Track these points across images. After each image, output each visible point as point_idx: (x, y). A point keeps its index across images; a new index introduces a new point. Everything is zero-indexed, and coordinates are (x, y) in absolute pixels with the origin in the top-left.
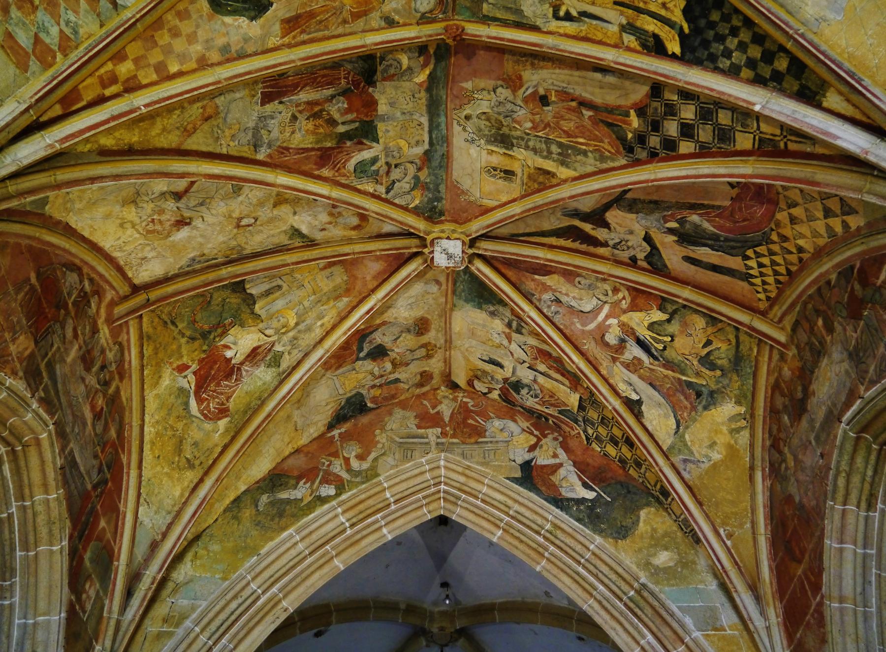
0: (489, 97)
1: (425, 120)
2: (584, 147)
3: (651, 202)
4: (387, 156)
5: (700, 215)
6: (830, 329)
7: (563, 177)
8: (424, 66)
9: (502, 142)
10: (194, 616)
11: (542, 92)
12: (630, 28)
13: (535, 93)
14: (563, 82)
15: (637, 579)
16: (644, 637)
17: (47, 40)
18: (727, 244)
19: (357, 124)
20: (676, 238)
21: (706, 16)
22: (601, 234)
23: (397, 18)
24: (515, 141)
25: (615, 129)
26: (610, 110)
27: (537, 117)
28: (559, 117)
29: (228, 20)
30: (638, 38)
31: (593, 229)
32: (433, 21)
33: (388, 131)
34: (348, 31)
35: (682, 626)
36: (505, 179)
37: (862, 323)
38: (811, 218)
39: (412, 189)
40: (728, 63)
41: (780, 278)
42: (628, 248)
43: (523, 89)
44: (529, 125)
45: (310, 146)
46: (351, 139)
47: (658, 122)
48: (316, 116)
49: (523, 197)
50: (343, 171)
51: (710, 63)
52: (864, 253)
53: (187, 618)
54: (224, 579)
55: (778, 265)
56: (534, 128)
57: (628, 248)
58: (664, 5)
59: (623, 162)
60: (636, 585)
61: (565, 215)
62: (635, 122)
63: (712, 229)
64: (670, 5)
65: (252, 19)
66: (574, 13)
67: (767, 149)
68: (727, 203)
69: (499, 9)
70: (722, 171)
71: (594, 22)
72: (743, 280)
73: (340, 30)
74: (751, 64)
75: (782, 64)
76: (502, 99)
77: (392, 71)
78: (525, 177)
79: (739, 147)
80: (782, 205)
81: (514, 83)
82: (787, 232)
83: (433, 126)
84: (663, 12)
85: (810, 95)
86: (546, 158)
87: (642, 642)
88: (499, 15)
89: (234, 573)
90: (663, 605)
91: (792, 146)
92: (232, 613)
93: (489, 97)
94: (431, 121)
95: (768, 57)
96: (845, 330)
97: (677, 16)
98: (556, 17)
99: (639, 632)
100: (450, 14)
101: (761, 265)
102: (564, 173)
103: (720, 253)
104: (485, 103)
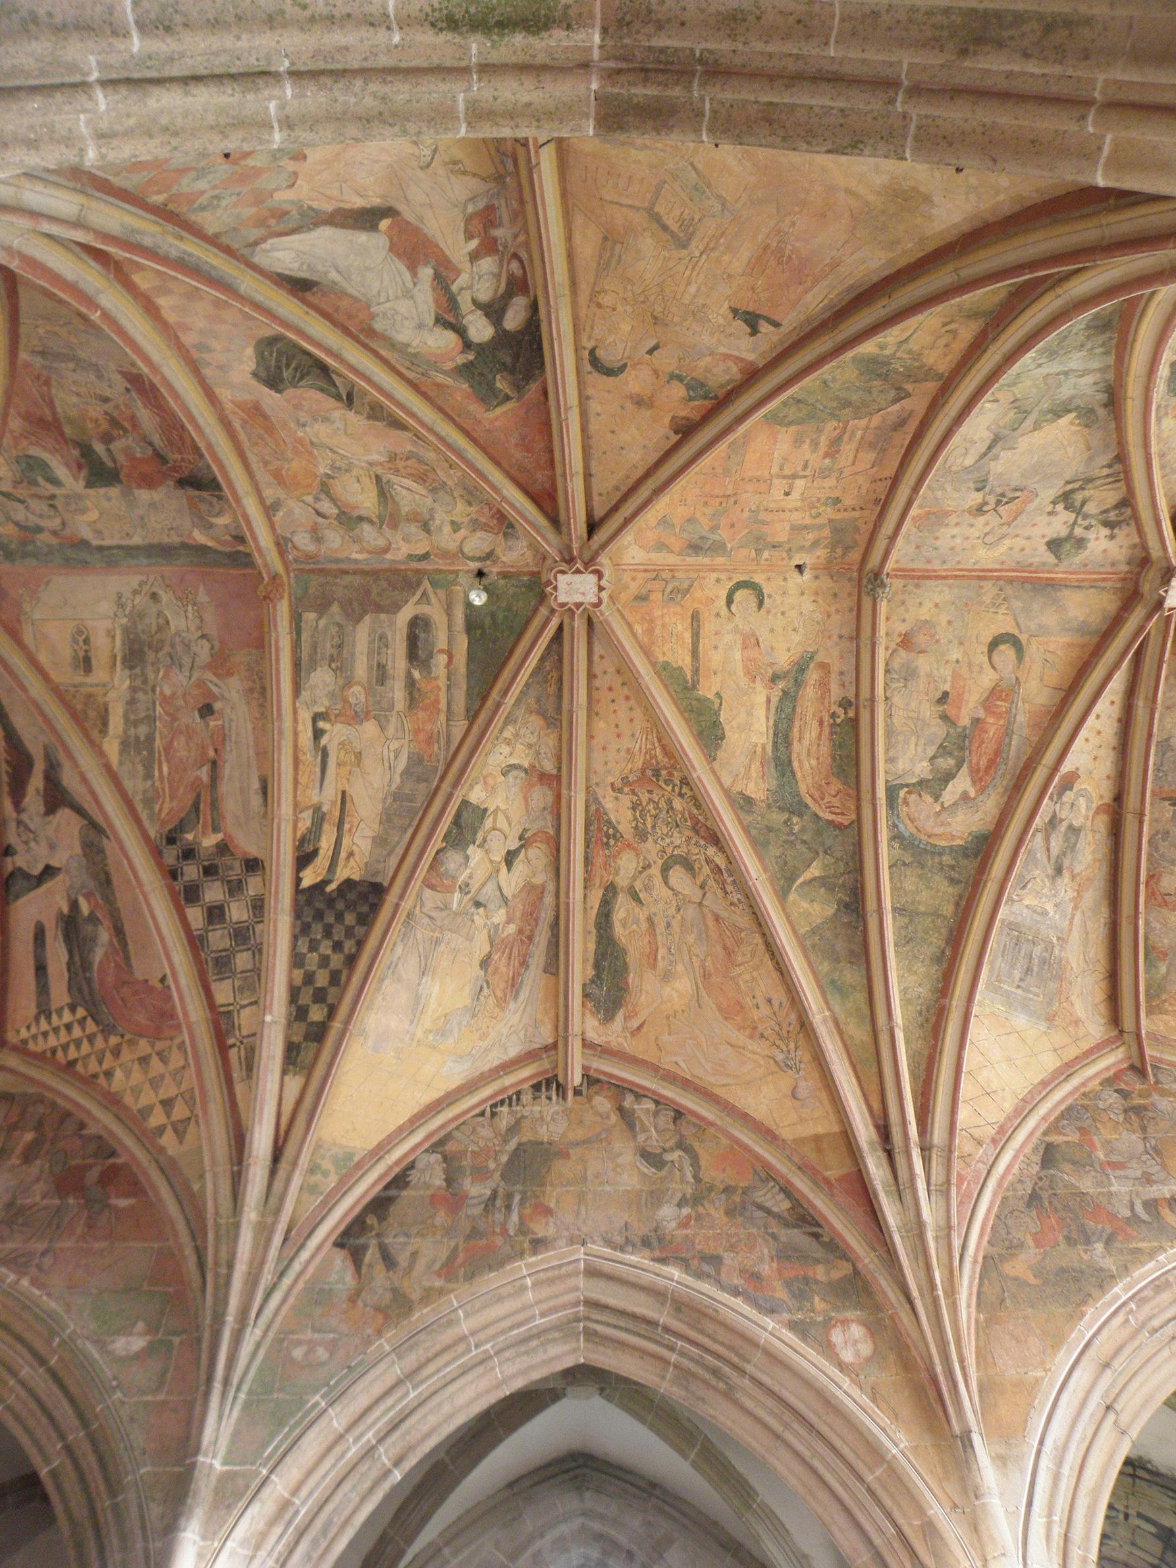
0: (192, 629)
1: (137, 540)
2: (156, 773)
3: (107, 874)
4: (66, 496)
5: (111, 943)
6: (29, 1156)
7: (106, 747)
8: (218, 541)
9: (132, 652)
11: (217, 706)
12: (319, 818)
13: (215, 698)
14: (237, 734)
17: (185, 181)
18: (84, 983)
19: (110, 464)
20: (66, 910)
21: (348, 907)
22: (33, 800)
23: (281, 514)
24: (138, 671)
25: (193, 816)
26: (215, 805)
27: (181, 702)
28: (189, 734)
29: (250, 351)
30: (309, 831)
31: (37, 791)
32: (282, 553)
33: (109, 499)
34: (255, 466)
36: (75, 658)
37: (57, 1201)
38: (155, 1083)
39: (17, 524)
40: (304, 950)
41: (60, 1054)
42: (26, 843)
43: (215, 679)
44: (168, 691)
45: (59, 410)
46: (83, 455)
47: (217, 873)
48: (114, 422)
49: (56, 691)
50: (25, 443)
51: (302, 929)
52: (138, 1164)
55: (78, 1047)
56: (165, 700)
57: (26, 843)
58: (351, 854)
59: (152, 833)
61: (45, 748)
62: (209, 841)
63: (97, 960)
64: (352, 862)
65: (255, 374)
66: (323, 741)
67: (222, 1025)
68: (139, 975)
69: (312, 636)
70: (183, 981)
71: (318, 770)
72: (39, 1006)
73: (252, 459)
74: (309, 979)
75: (317, 1014)
76: (194, 648)
77: (203, 507)
78: (90, 690)
79: (215, 987)
80: (160, 1045)
81: (220, 664)
82: (127, 1055)
83: (131, 551)
84: (343, 855)
85: (292, 1053)
86: (126, 717)
88: (304, 636)
91: (233, 1054)
93: (192, 629)
94: (137, 548)
95: (320, 996)
96: (38, 1179)
97: (342, 874)
98: (316, 718)
100: (295, 566)
101: (68, 1027)
102: (112, 748)
103: (66, 975)
104: (182, 624)
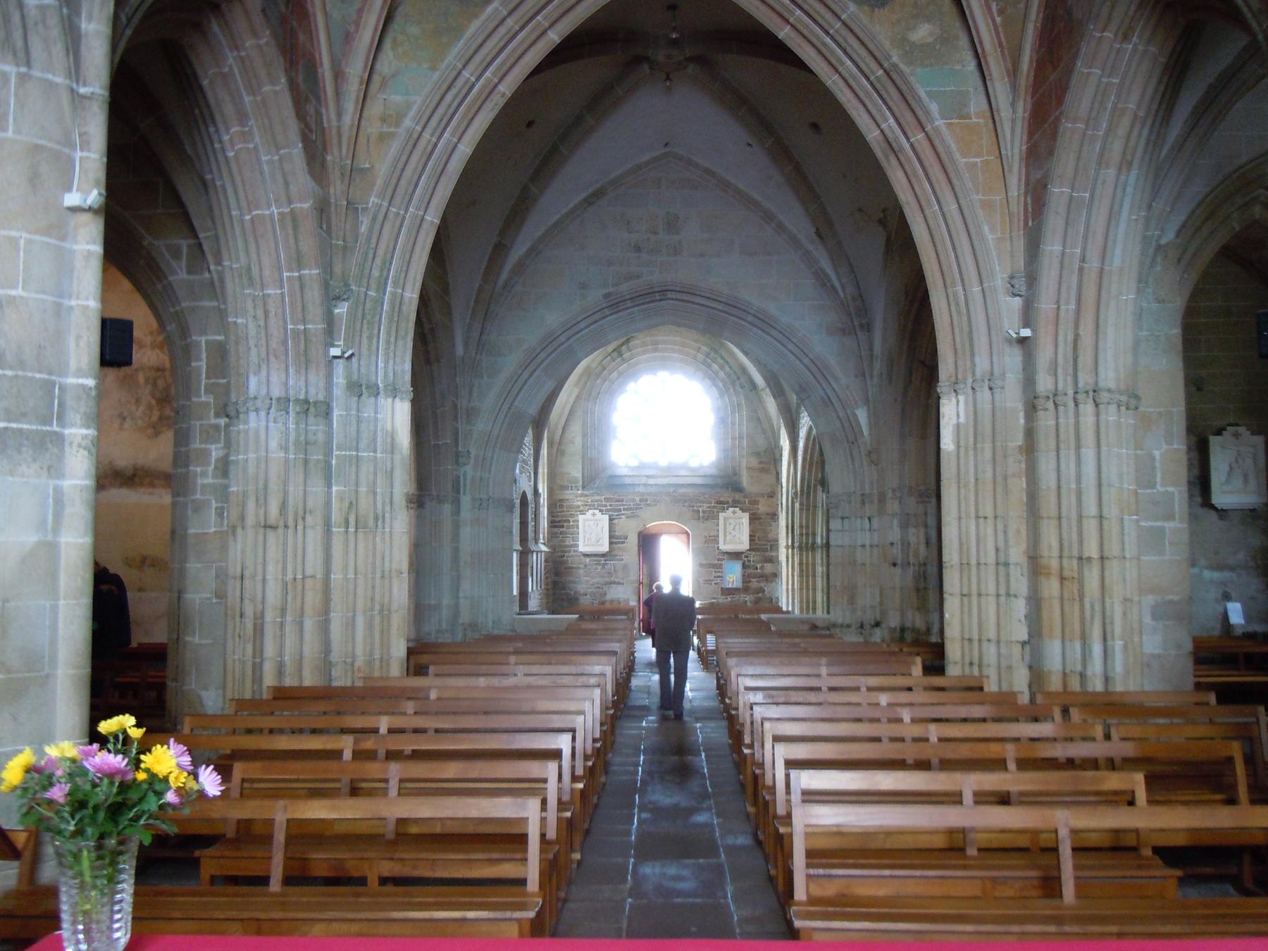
10: (412, 114)
15: (888, 57)
16: (886, 120)
35: (927, 113)
53: (405, 116)
54: (433, 69)
60: (886, 65)
87: (883, 126)
89: (443, 61)
90: (911, 89)
92: (450, 106)
99: (883, 115)
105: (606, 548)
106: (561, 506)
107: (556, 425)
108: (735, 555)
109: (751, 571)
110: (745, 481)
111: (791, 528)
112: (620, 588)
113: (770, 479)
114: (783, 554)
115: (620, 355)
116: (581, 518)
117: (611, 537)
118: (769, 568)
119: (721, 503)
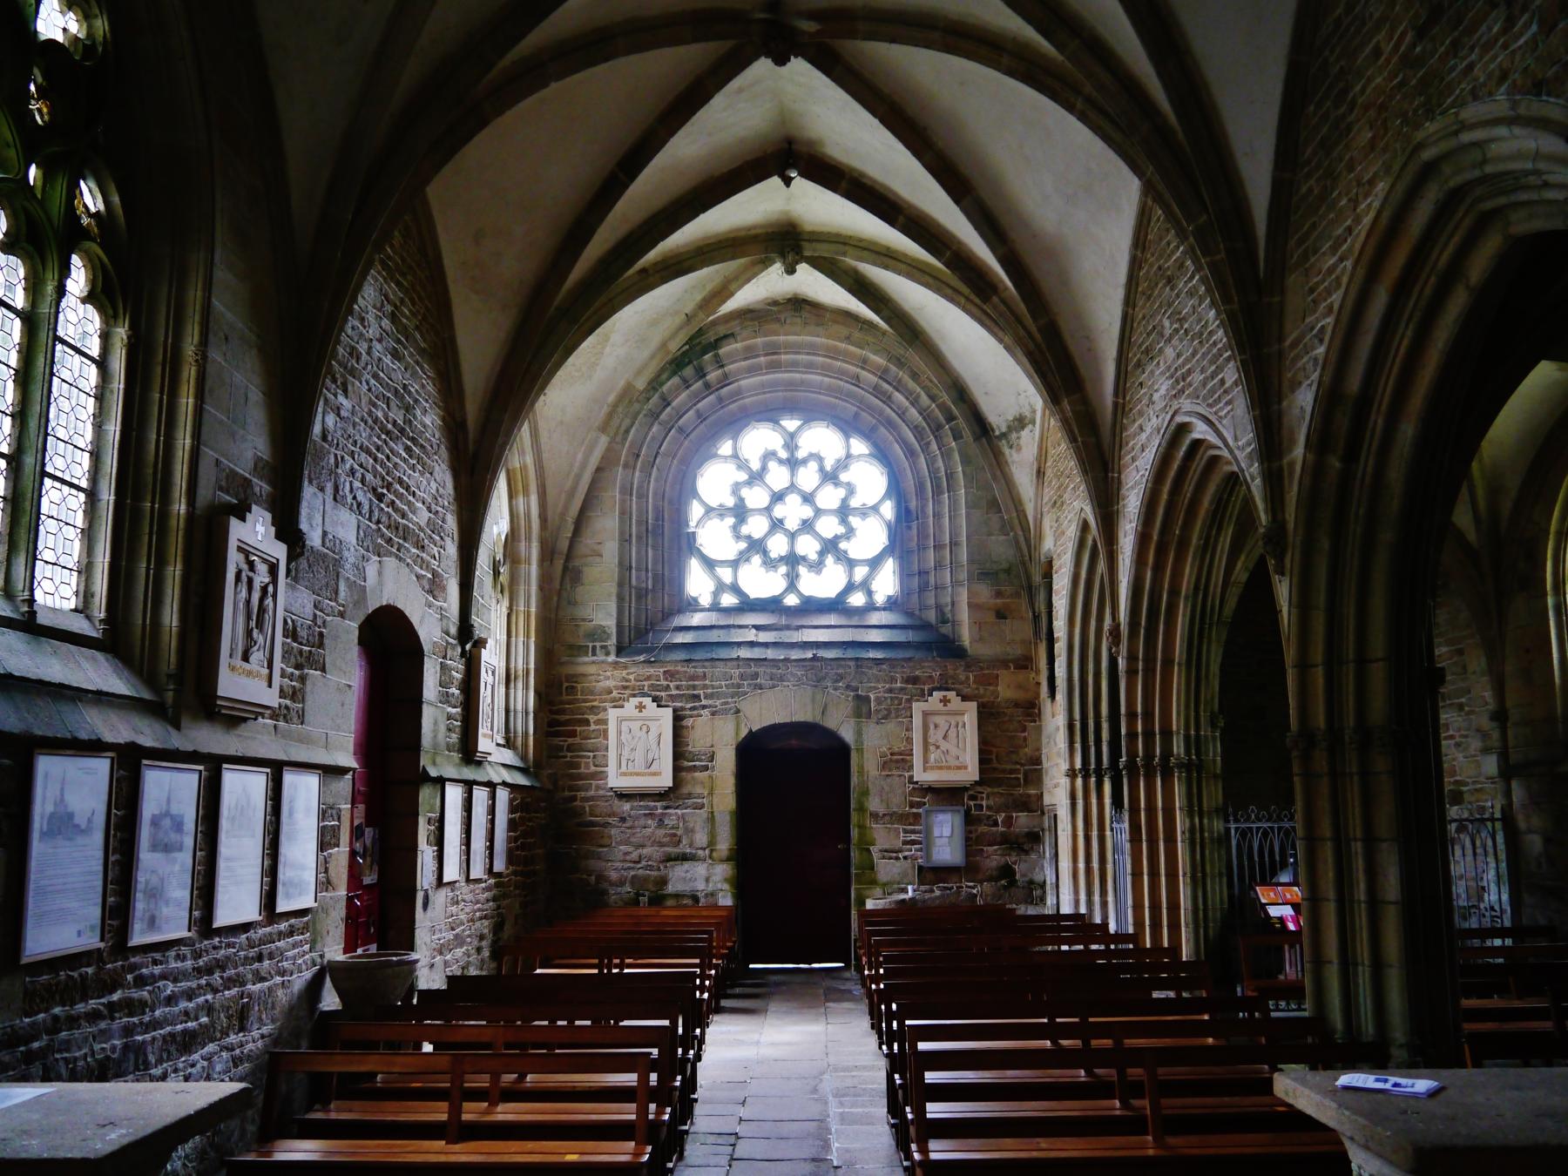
105: (666, 781)
106: (572, 690)
107: (563, 515)
108: (947, 795)
109: (983, 829)
110: (966, 636)
111: (1080, 731)
112: (700, 869)
113: (1019, 629)
114: (1057, 791)
115: (701, 373)
116: (613, 714)
117: (678, 755)
118: (1022, 820)
119: (914, 680)
